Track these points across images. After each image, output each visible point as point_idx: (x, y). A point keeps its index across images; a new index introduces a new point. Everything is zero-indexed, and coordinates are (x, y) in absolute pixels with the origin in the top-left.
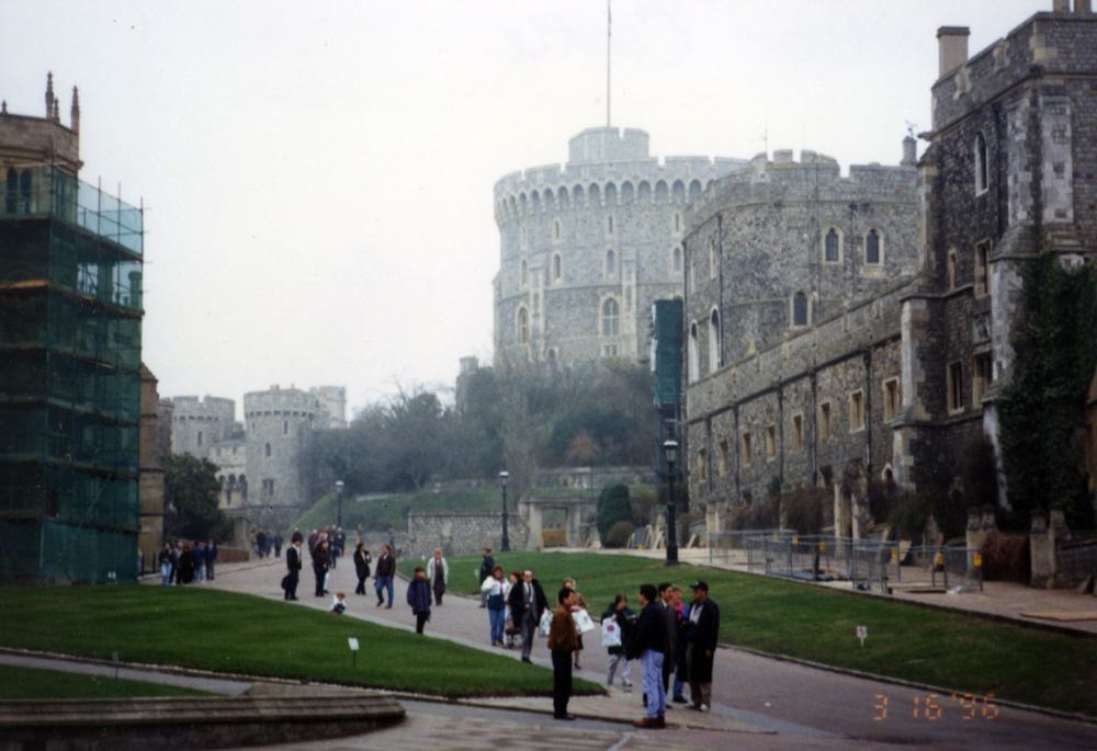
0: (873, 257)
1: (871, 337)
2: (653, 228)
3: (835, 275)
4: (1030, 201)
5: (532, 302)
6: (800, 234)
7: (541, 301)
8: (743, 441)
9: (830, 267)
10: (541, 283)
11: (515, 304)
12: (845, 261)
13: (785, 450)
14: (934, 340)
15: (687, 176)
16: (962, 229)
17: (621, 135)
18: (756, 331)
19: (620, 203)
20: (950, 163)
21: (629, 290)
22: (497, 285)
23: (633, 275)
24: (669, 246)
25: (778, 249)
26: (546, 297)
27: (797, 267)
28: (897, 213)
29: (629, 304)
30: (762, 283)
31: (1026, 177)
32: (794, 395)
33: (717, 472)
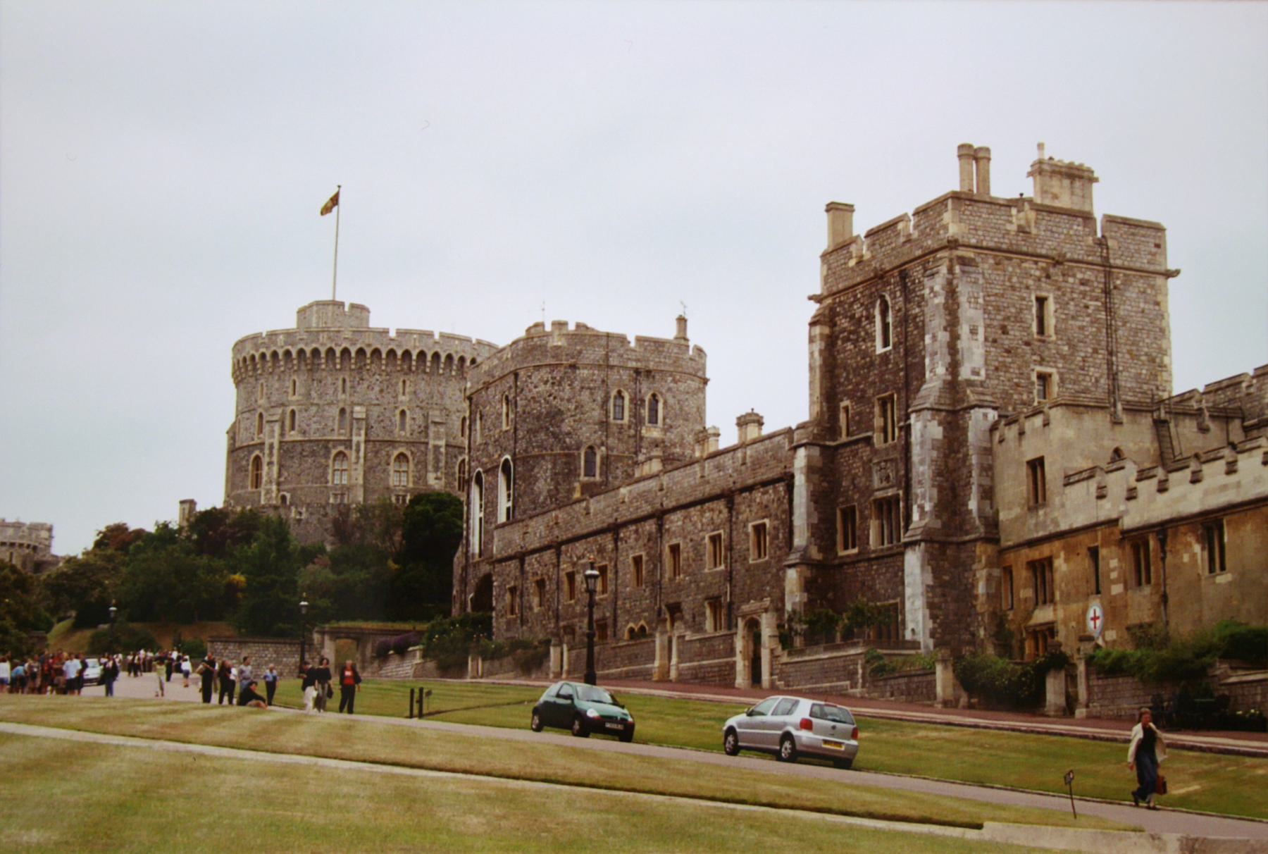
0: (653, 419)
1: (734, 483)
2: (381, 391)
3: (620, 433)
4: (948, 359)
5: (267, 451)
6: (592, 394)
7: (275, 451)
8: (565, 579)
9: (617, 425)
10: (277, 434)
11: (250, 453)
12: (630, 421)
13: (620, 588)
14: (825, 484)
15: (415, 347)
16: (858, 384)
17: (347, 309)
18: (549, 480)
19: (353, 367)
20: (844, 323)
21: (358, 445)
22: (231, 434)
23: (363, 432)
24: (396, 408)
25: (572, 407)
26: (280, 448)
27: (588, 424)
28: (675, 381)
29: (358, 458)
30: (555, 435)
31: (944, 337)
32: (633, 536)
33: (531, 608)
